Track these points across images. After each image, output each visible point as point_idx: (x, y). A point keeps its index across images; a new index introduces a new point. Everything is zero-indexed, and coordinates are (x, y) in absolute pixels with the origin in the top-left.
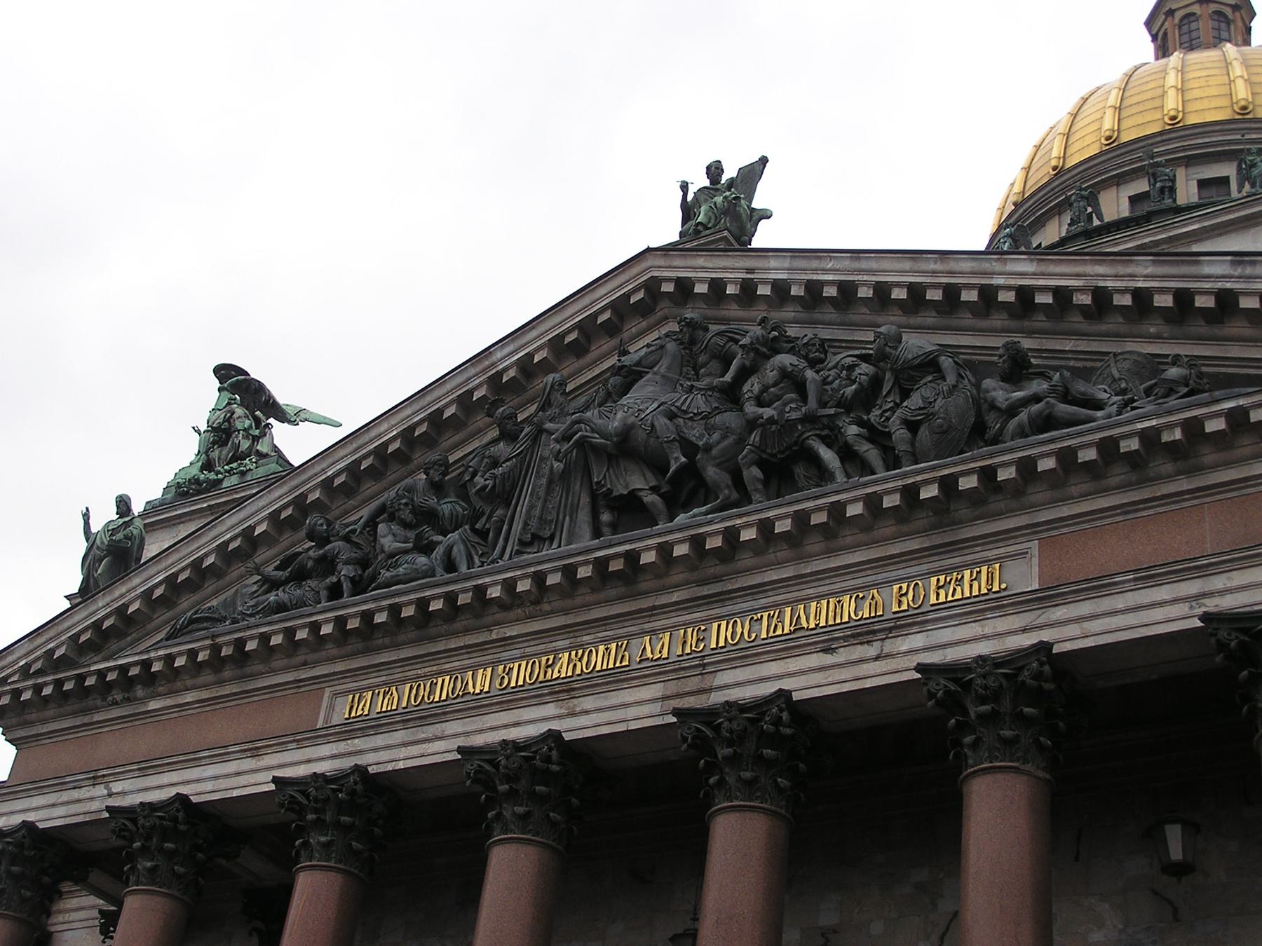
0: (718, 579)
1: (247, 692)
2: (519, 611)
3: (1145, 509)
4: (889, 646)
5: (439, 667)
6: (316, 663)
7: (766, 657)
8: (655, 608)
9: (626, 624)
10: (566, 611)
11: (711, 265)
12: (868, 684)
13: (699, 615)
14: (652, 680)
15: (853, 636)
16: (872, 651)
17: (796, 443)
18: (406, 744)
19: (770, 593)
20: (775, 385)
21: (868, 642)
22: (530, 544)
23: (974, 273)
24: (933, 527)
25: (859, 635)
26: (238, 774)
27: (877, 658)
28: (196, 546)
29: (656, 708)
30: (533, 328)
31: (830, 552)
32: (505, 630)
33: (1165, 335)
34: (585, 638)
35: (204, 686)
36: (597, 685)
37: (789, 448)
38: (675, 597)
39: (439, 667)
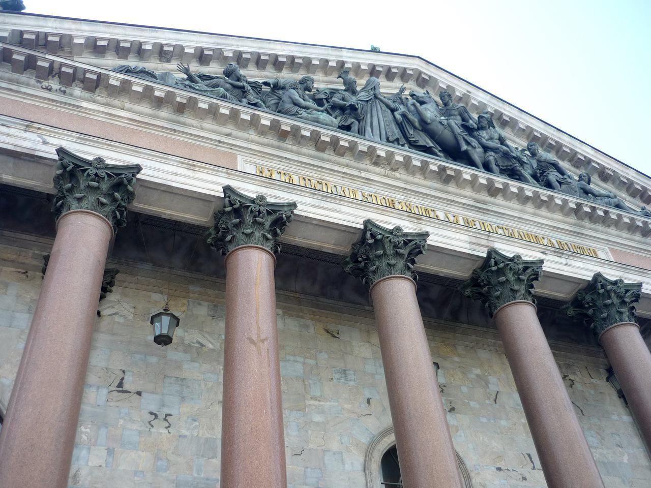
0: (485, 203)
1: (175, 130)
2: (382, 170)
3: (643, 253)
4: (569, 262)
5: (322, 177)
6: (237, 138)
7: (516, 244)
8: (453, 201)
9: (435, 202)
10: (406, 182)
11: (450, 80)
12: (565, 273)
13: (471, 214)
14: (462, 232)
15: (555, 252)
16: (563, 261)
17: (511, 166)
18: (313, 206)
19: (505, 220)
20: (496, 139)
21: (560, 257)
22: (393, 142)
23: (569, 143)
24: (575, 225)
25: (557, 252)
26: (176, 174)
27: (566, 265)
28: (141, 34)
29: (467, 246)
30: (363, 54)
31: (534, 214)
32: (370, 176)
33: (627, 199)
34: (412, 199)
35: (139, 113)
36: (434, 223)
37: (507, 166)
38: (464, 201)
39: (322, 177)
